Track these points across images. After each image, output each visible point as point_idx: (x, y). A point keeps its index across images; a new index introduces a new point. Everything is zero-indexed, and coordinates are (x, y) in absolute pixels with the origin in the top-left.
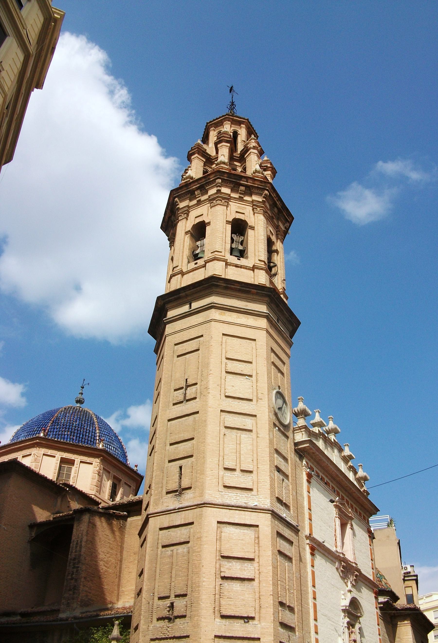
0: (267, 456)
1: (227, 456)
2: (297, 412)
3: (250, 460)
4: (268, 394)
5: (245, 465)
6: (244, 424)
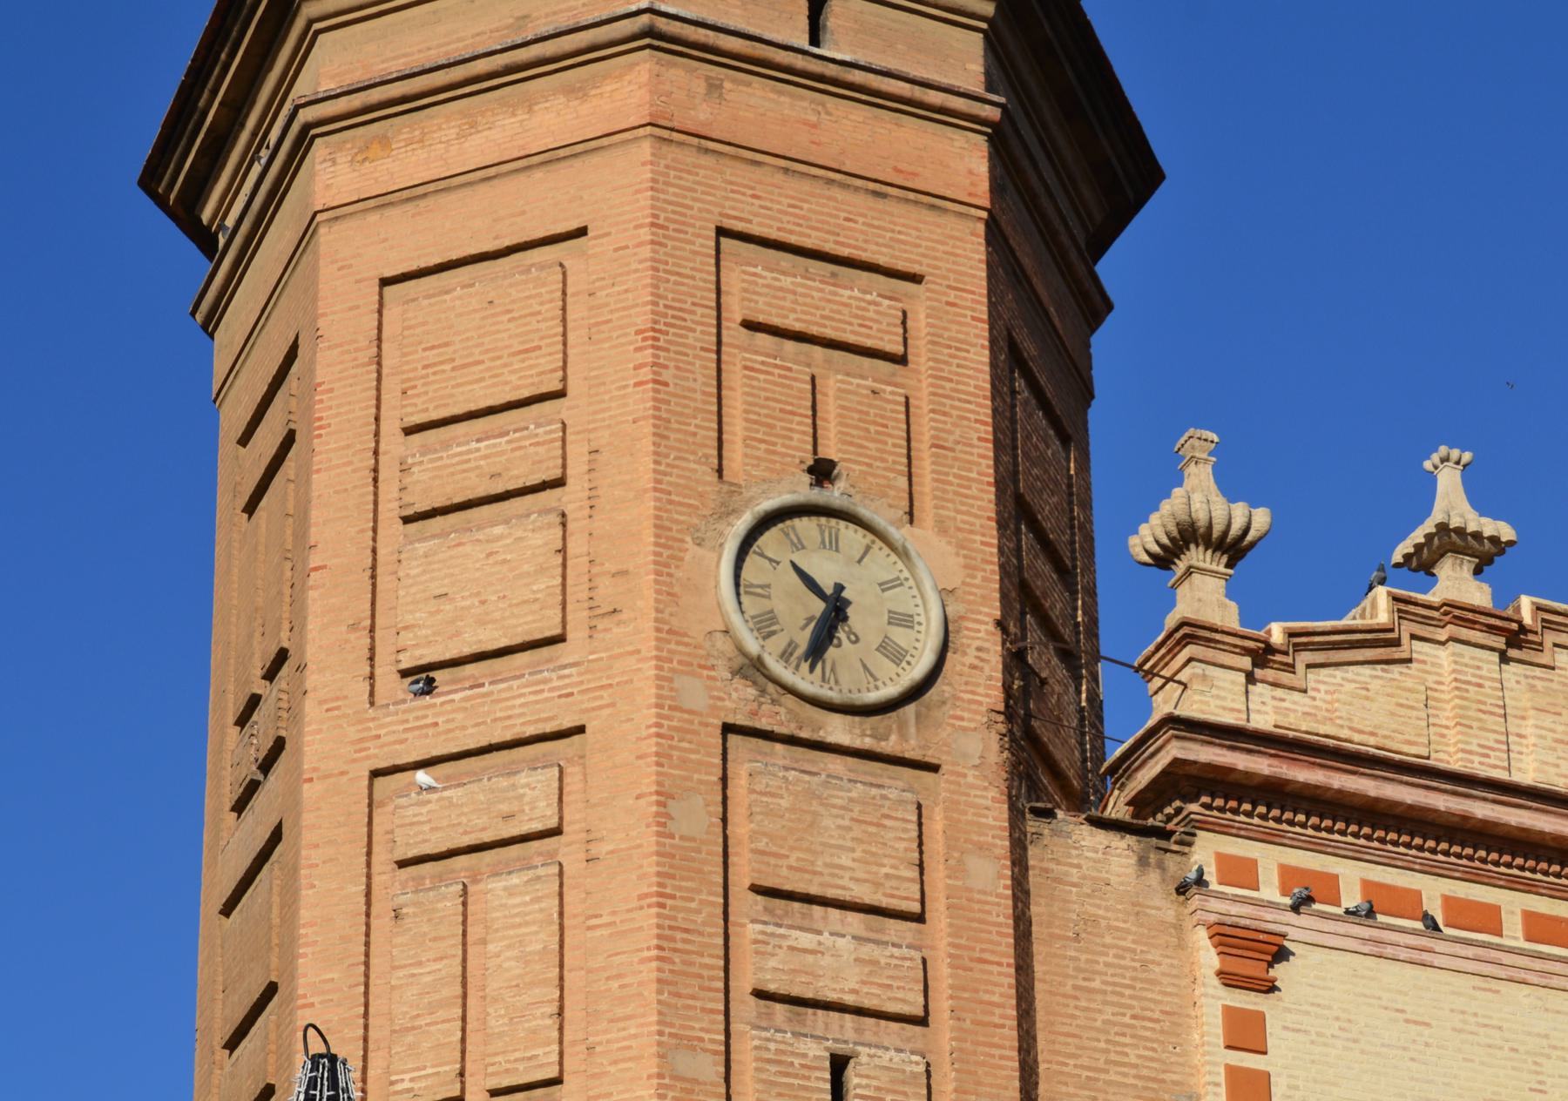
0: (643, 961)
1: (410, 1038)
2: (1165, 541)
3: (543, 1016)
4: (663, 568)
5: (517, 1055)
6: (504, 808)
